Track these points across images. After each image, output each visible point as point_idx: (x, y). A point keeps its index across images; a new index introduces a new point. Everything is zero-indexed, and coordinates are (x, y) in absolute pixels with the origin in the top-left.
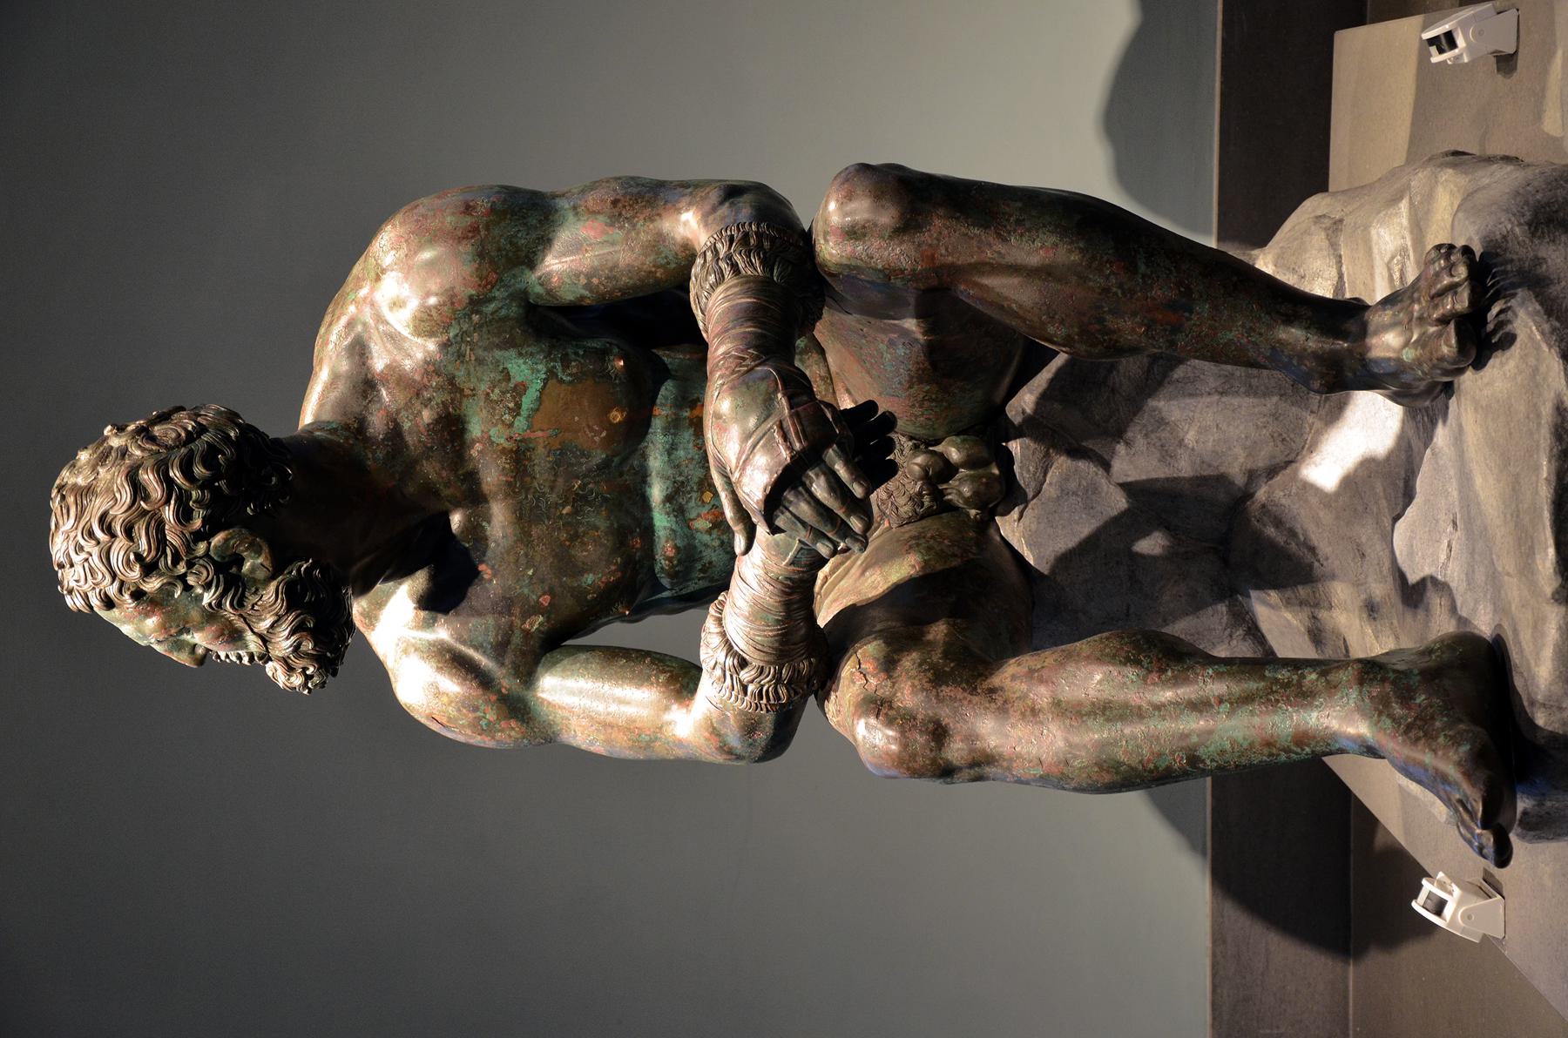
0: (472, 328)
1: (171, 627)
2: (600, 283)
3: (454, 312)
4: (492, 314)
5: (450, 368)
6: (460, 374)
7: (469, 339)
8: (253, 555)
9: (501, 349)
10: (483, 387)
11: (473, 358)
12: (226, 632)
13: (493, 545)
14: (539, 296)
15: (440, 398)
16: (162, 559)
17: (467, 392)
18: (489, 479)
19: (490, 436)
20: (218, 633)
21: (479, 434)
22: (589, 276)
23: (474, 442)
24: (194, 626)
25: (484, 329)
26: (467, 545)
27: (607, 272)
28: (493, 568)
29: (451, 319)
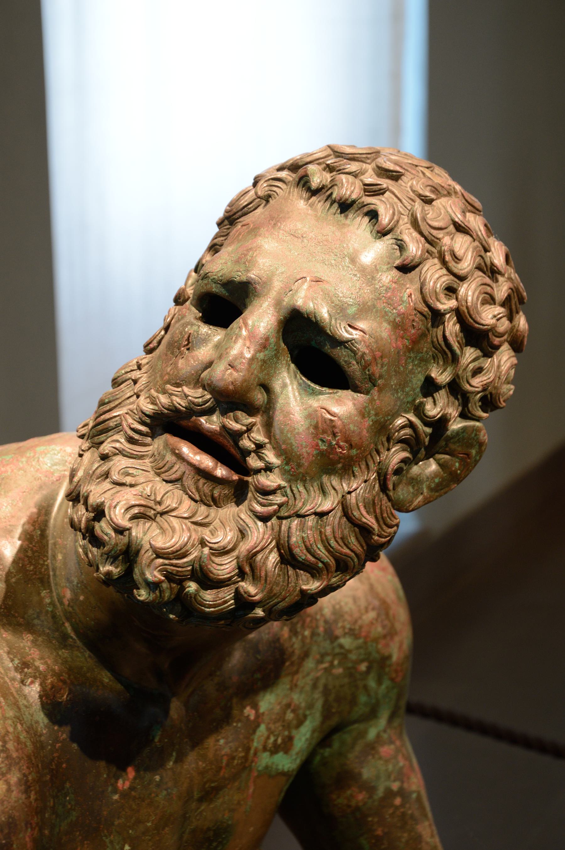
0: (350, 665)
1: (382, 366)
2: (397, 808)
3: (376, 640)
4: (365, 687)
5: (315, 649)
6: (310, 664)
7: (336, 662)
8: (437, 480)
9: (324, 706)
10: (297, 698)
11: (319, 674)
12: (354, 452)
13: (157, 778)
14: (363, 734)
15: (296, 643)
16: (478, 353)
17: (296, 677)
18: (222, 742)
19: (258, 726)
20: (355, 440)
21: (262, 710)
22: (401, 792)
23: (255, 706)
24: (372, 400)
25: (346, 680)
26: (157, 740)
27: (410, 812)
28: (132, 788)
29: (366, 637)
